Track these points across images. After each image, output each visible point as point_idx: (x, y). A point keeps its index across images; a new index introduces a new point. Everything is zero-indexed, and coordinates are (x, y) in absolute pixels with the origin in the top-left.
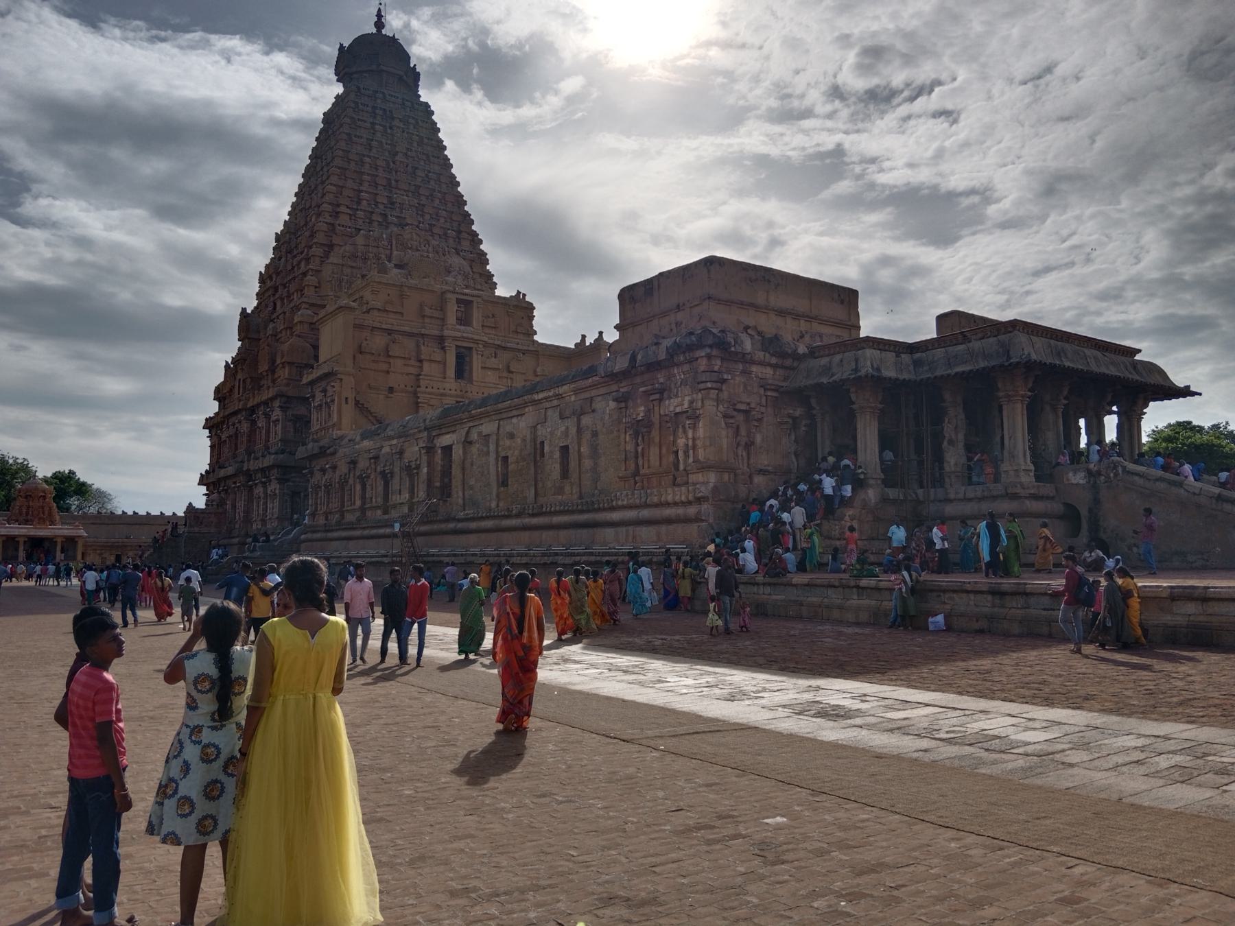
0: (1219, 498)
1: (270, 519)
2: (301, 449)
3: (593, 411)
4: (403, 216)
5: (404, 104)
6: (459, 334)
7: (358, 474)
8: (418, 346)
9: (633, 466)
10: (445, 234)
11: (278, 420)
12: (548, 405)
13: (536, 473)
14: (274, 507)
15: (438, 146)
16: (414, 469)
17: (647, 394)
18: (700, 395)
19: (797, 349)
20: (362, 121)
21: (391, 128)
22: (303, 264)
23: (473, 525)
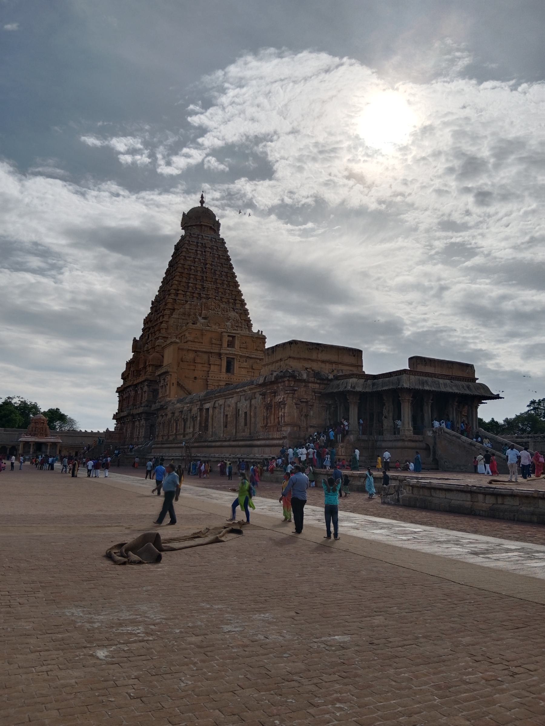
2: (153, 406)
4: (208, 294)
5: (212, 240)
6: (228, 352)
7: (175, 418)
8: (209, 357)
9: (265, 422)
10: (228, 301)
11: (146, 391)
12: (241, 394)
14: (143, 432)
15: (227, 259)
17: (271, 393)
18: (286, 396)
21: (205, 252)
22: (161, 318)
23: (214, 444)
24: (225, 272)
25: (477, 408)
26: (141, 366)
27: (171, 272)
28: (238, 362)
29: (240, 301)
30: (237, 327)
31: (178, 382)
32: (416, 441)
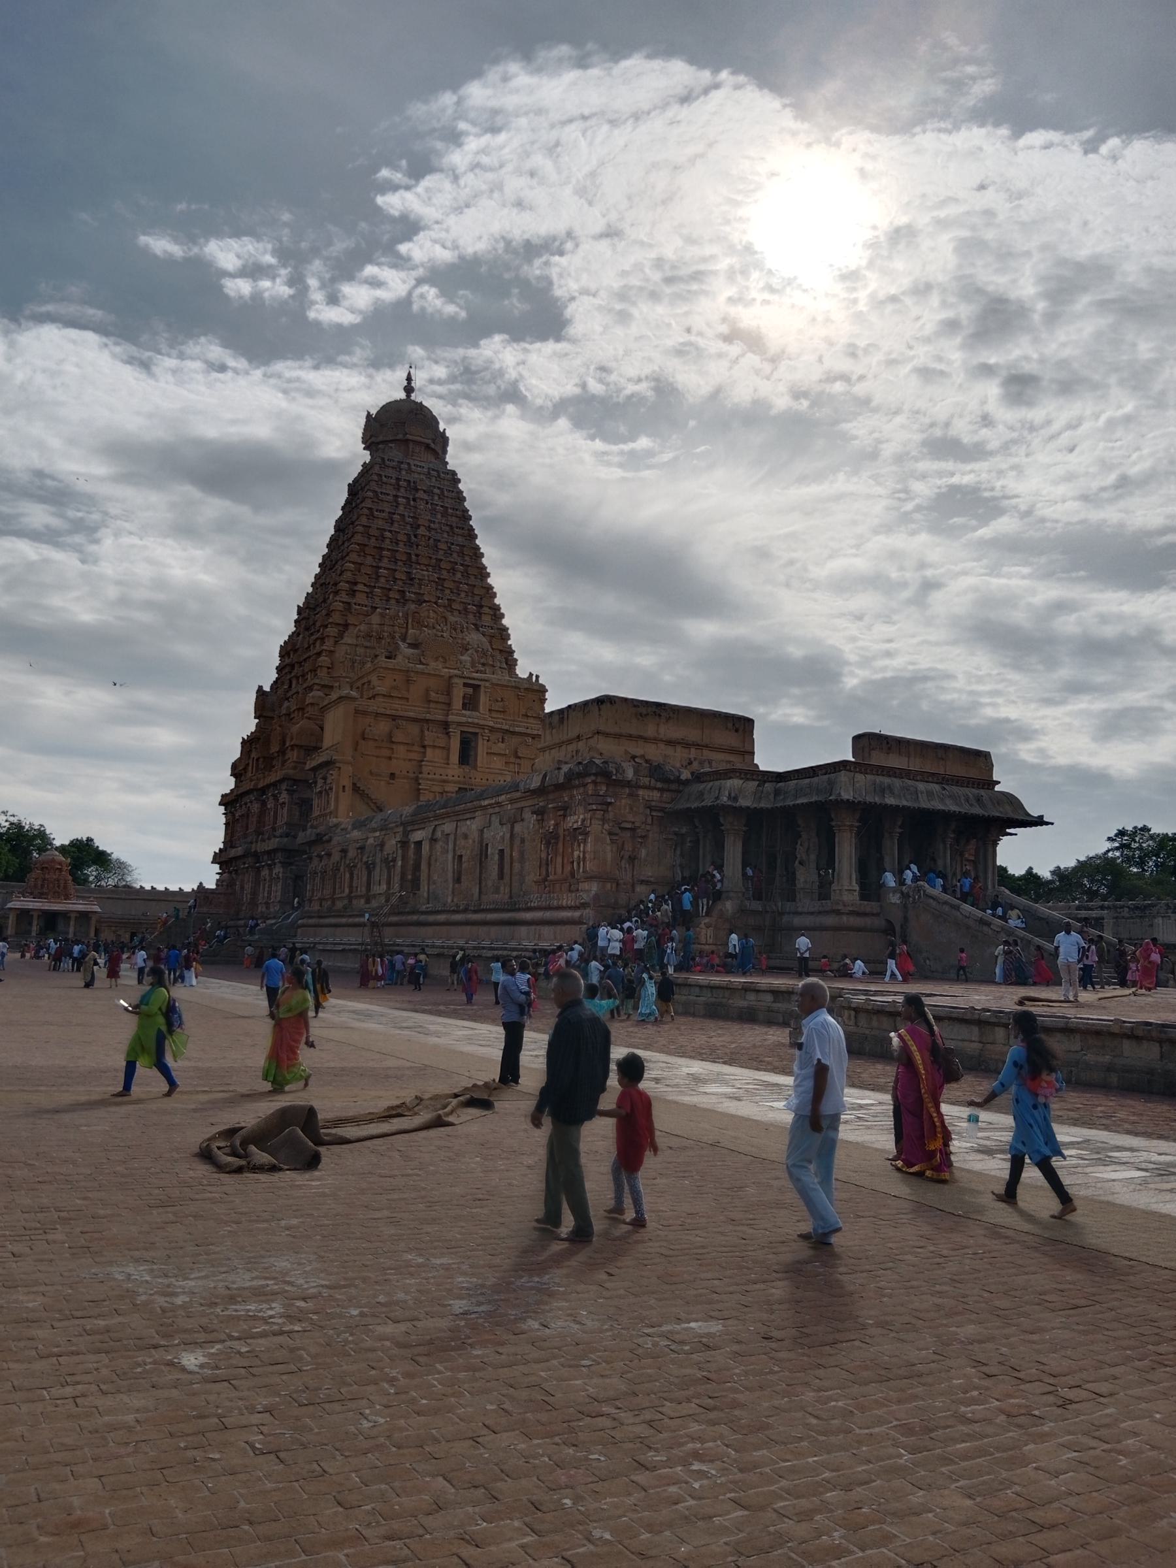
2: (301, 834)
3: (522, 820)
5: (429, 473)
6: (464, 719)
7: (348, 862)
8: (422, 731)
9: (544, 873)
10: (466, 609)
11: (284, 803)
12: (491, 811)
13: (481, 873)
14: (277, 891)
17: (557, 809)
18: (588, 815)
21: (414, 500)
22: (318, 644)
23: (431, 918)
25: (995, 844)
26: (274, 748)
27: (340, 542)
28: (485, 742)
29: (490, 608)
30: (484, 665)
31: (354, 784)
32: (865, 914)
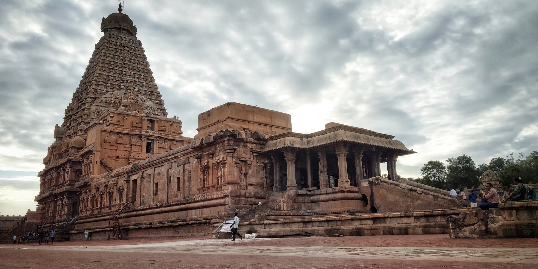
0: (411, 190)
1: (63, 215)
2: (77, 183)
4: (127, 85)
5: (129, 41)
6: (148, 134)
7: (99, 193)
8: (130, 139)
12: (173, 161)
13: (168, 189)
14: (65, 210)
15: (144, 58)
16: (121, 190)
17: (208, 155)
19: (265, 137)
20: (111, 47)
21: (123, 50)
22: (83, 106)
23: (143, 212)
24: (141, 68)
26: (63, 150)
27: (92, 67)
28: (157, 143)
29: (155, 93)
